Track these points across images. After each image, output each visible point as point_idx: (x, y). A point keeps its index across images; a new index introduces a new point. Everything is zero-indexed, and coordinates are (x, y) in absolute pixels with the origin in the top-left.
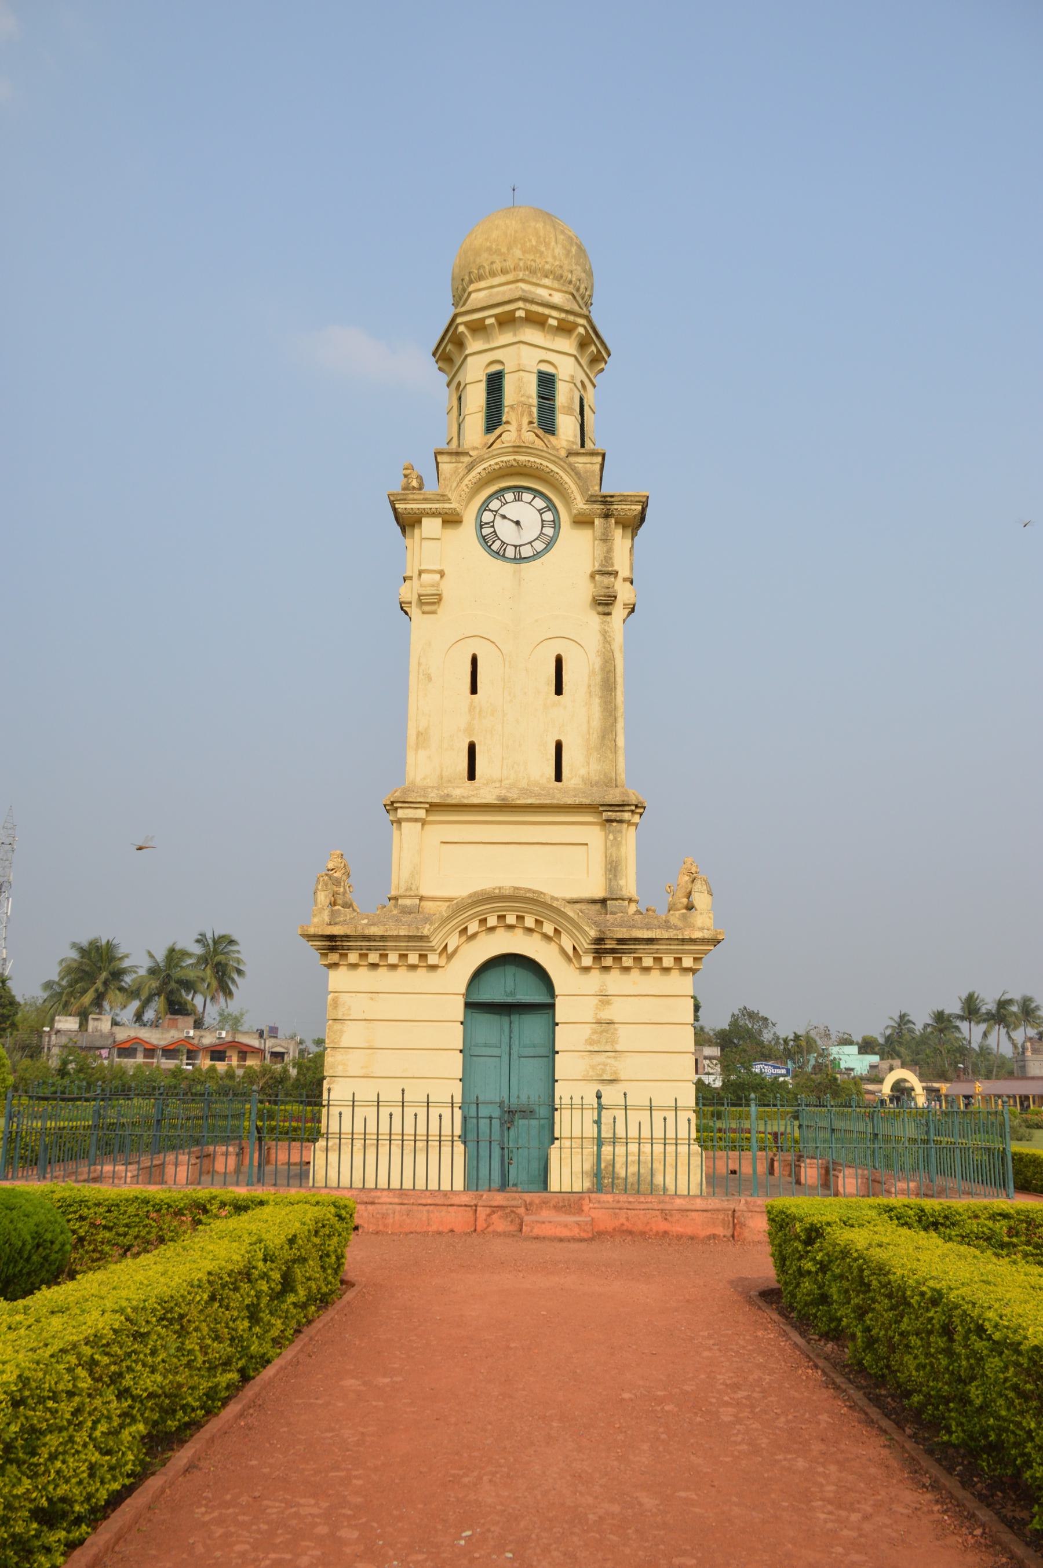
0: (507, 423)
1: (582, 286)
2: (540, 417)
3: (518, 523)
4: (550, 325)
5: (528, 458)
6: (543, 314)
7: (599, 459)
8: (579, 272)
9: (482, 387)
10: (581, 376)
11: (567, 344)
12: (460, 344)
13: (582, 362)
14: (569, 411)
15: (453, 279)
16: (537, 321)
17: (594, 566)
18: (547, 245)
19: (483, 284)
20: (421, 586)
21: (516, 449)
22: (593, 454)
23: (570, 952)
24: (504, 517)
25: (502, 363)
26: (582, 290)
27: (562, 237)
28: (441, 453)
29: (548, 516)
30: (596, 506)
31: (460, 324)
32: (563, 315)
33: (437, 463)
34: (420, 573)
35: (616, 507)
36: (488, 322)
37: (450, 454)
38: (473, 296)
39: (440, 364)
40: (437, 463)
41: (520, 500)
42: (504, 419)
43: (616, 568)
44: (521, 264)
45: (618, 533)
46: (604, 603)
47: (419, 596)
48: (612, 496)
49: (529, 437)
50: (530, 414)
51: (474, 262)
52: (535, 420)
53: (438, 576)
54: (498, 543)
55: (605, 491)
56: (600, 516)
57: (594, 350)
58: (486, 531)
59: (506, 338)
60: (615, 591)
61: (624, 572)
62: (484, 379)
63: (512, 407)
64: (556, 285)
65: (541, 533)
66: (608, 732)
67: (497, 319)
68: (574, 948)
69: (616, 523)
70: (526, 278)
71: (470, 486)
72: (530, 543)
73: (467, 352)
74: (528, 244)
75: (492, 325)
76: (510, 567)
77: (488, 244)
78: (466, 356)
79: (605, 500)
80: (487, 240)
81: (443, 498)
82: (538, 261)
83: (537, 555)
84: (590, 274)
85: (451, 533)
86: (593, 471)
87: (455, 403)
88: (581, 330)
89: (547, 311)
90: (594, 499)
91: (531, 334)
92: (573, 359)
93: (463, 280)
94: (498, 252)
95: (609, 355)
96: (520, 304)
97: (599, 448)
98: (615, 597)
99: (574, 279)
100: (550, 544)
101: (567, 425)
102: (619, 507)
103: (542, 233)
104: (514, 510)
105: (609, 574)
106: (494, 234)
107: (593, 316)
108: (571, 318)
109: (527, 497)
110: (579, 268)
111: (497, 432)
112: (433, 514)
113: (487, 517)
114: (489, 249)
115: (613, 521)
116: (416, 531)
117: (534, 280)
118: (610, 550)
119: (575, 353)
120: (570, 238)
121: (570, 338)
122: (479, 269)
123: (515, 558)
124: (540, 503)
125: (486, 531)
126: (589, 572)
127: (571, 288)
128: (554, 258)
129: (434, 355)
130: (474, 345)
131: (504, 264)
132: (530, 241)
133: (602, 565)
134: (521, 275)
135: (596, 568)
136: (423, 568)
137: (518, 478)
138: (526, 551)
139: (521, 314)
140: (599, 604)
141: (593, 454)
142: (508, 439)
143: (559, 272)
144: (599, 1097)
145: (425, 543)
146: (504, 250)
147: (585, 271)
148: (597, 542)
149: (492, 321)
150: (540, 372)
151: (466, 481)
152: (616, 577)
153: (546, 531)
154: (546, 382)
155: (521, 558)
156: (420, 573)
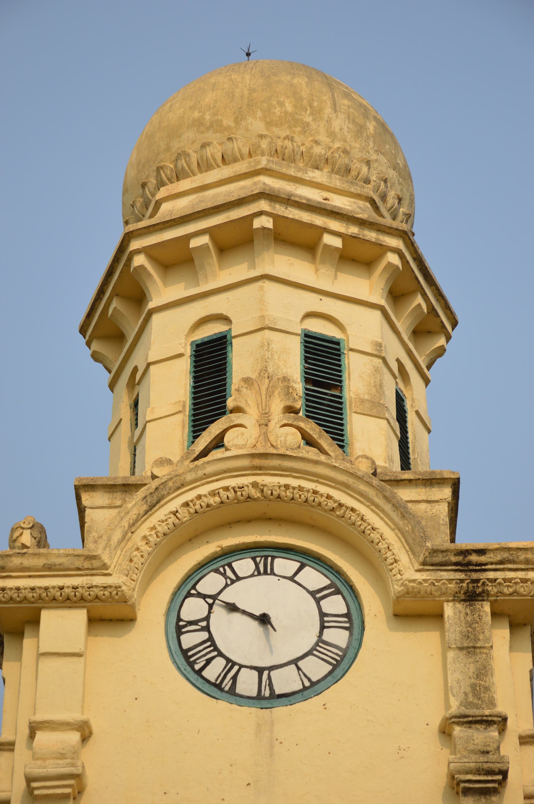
0: (238, 410)
1: (391, 195)
2: (309, 396)
3: (264, 620)
4: (326, 246)
5: (284, 481)
6: (311, 226)
7: (447, 492)
8: (382, 166)
9: (185, 365)
10: (395, 351)
11: (369, 287)
12: (138, 298)
13: (399, 325)
14: (374, 409)
15: (125, 191)
16: (303, 242)
17: (448, 706)
18: (317, 113)
19: (185, 185)
20: (35, 758)
21: (257, 462)
22: (431, 481)
24: (232, 608)
25: (226, 319)
26: (391, 200)
27: (346, 102)
28: (91, 487)
29: (335, 605)
30: (445, 575)
31: (138, 252)
32: (354, 230)
33: (82, 511)
34: (34, 729)
35: (491, 575)
36: (194, 243)
37: (111, 488)
38: (165, 207)
39: (96, 346)
40: (82, 511)
41: (268, 571)
42: (230, 403)
43: (501, 708)
44: (264, 144)
45: (500, 636)
47: (29, 780)
48: (481, 552)
49: (288, 438)
50: (288, 391)
51: (168, 149)
52: (299, 404)
53: (75, 737)
54: (219, 664)
55: (464, 541)
56: (455, 598)
57: (424, 311)
58: (189, 640)
59: (238, 271)
60: (503, 760)
61: (521, 722)
62: (188, 351)
63: (247, 381)
64: (337, 182)
65: (320, 640)
67: (213, 238)
69: (494, 614)
70: (274, 167)
71: (153, 539)
72: (295, 662)
73: (151, 305)
74: (277, 110)
75: (203, 248)
76: (249, 714)
77: (196, 114)
78: (151, 313)
79: (467, 561)
80: (192, 108)
81: (93, 565)
82: (297, 138)
83: (311, 688)
84: (406, 176)
85: (109, 646)
86: (434, 518)
87: (126, 413)
88: (393, 259)
89: (319, 221)
90: (439, 558)
92: (378, 314)
93: (144, 185)
94: (216, 126)
95: (454, 324)
96: (263, 205)
97: (446, 470)
98: (504, 774)
99: (373, 178)
100: (341, 664)
101: (370, 437)
102: (499, 575)
103: (305, 93)
104: (253, 592)
105: (486, 722)
106: (209, 98)
107: (417, 239)
108: (371, 235)
109: (285, 566)
110: (381, 158)
111: (214, 429)
112: (67, 601)
113: (194, 609)
114: (198, 124)
115: (487, 608)
116: (28, 643)
117: (292, 172)
118: (483, 672)
119: (382, 302)
120: (365, 112)
121: (370, 275)
122: (177, 159)
123: (259, 697)
124: (313, 578)
125: (189, 640)
126: (436, 722)
127: (368, 190)
128: (332, 135)
129: (83, 330)
130: (162, 291)
131: (229, 145)
132: (281, 104)
133: (466, 704)
134: (263, 162)
135: (455, 707)
136: (39, 717)
137: (262, 527)
138: (286, 681)
139: (267, 222)
140: (466, 792)
141: (431, 481)
142: (240, 441)
143: (344, 160)
145: (46, 664)
146: (228, 122)
147: (395, 167)
148: (451, 655)
149: (205, 240)
151: (144, 529)
152: (502, 731)
153: (329, 635)
154: (323, 358)
156: (34, 729)
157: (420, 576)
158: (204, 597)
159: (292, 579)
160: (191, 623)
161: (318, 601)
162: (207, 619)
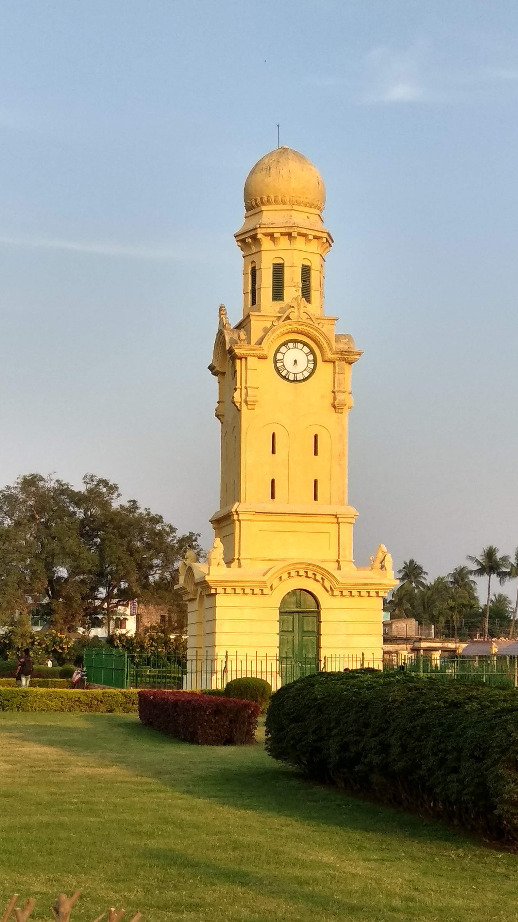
9: (271, 270)
23: (329, 589)
54: (285, 372)
62: (272, 267)
68: (331, 587)
72: (302, 372)
91: (300, 243)
101: (315, 294)
109: (300, 346)
144: (363, 654)
150: (303, 265)
155: (297, 381)
157: (332, 356)
158: (282, 353)
159: (301, 350)
160: (280, 360)
161: (307, 356)
162: (283, 359)
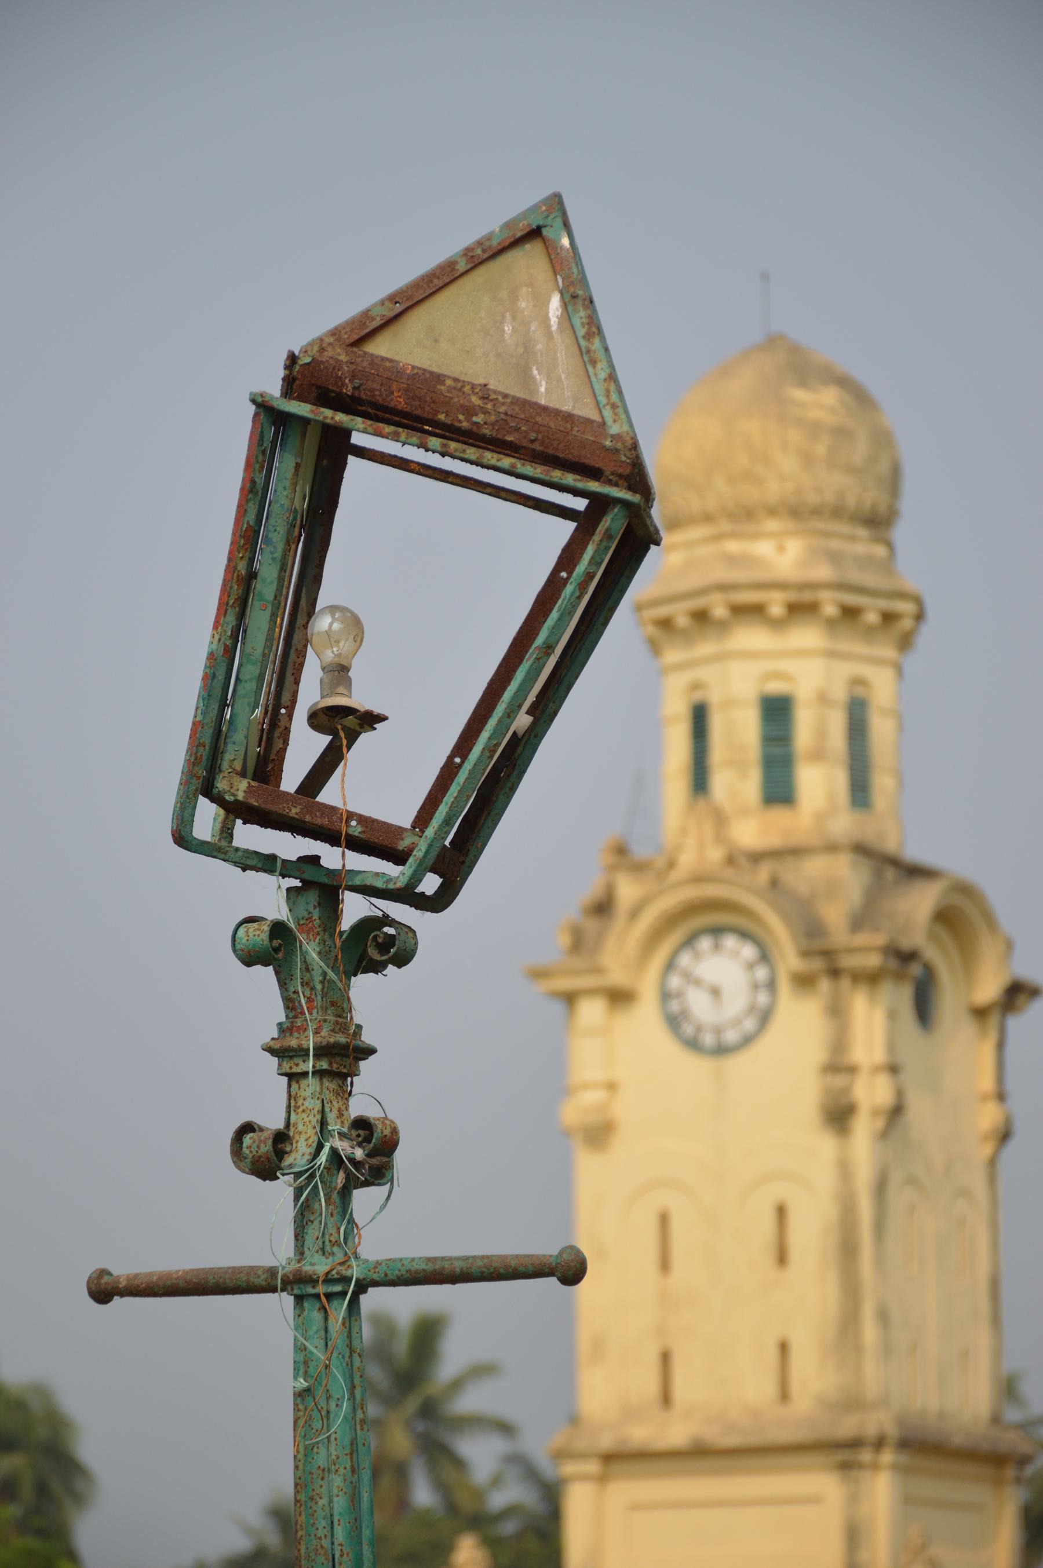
29: (762, 973)
46: (839, 1116)
58: (675, 1006)
66: (849, 1321)
83: (747, 1041)
109: (730, 942)
112: (591, 992)
124: (749, 951)
138: (731, 1036)
